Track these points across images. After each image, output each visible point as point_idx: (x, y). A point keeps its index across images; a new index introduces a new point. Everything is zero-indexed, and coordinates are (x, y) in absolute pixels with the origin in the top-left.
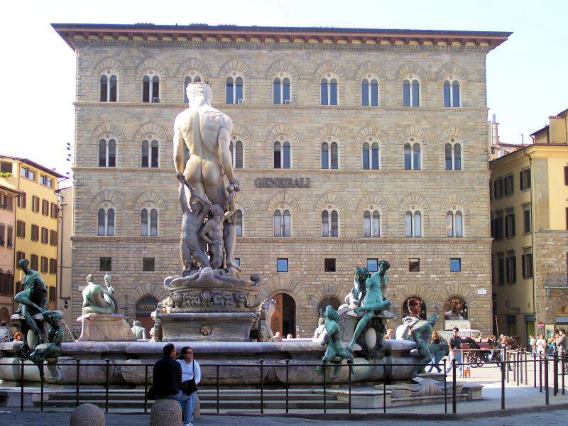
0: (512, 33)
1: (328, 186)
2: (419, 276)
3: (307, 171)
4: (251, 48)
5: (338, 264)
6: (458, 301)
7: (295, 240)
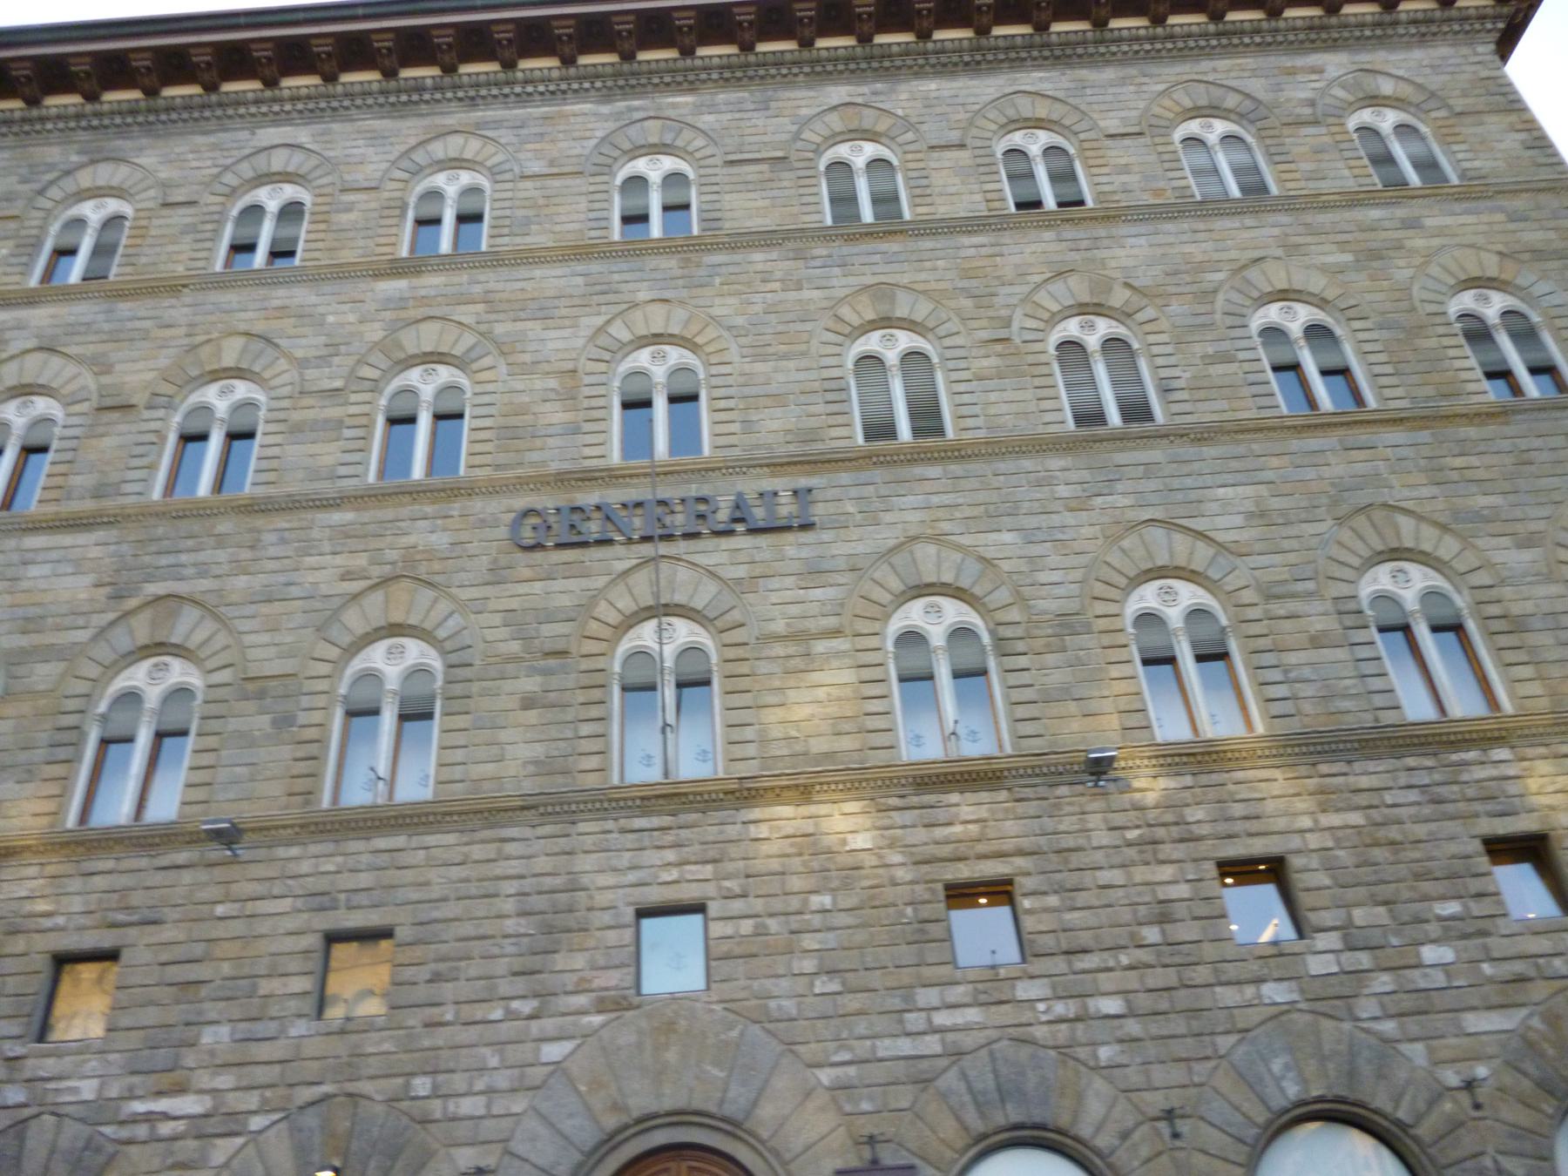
1: (908, 511)
4: (523, 99)
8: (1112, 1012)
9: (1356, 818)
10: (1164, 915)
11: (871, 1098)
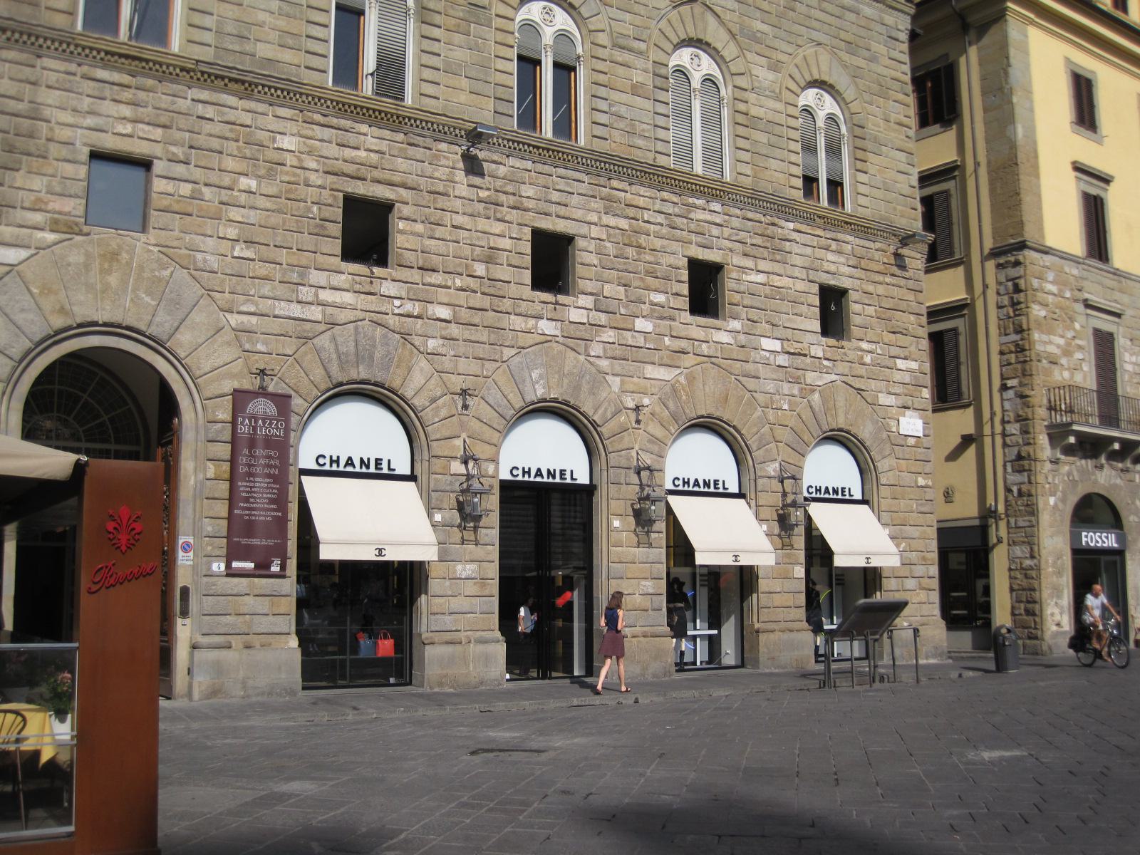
2: (723, 337)
8: (443, 317)
9: (624, 223)
10: (489, 261)
11: (265, 343)
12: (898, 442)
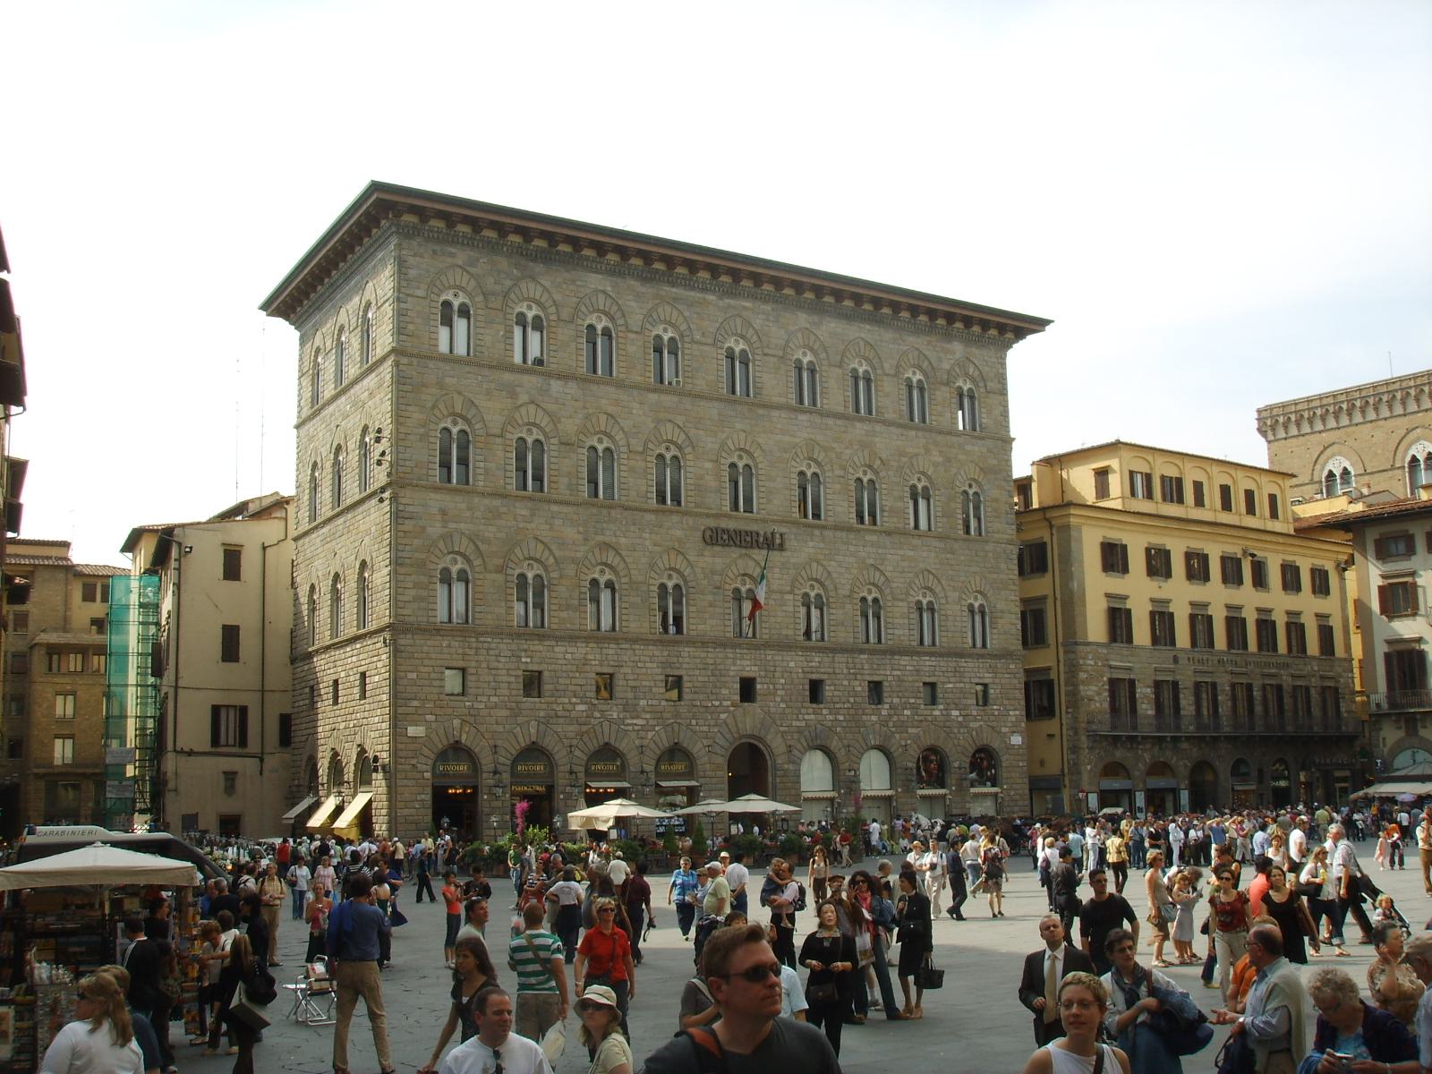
0: (1038, 324)
2: (937, 713)
3: (782, 521)
4: (693, 288)
5: (828, 690)
6: (983, 755)
7: (767, 645)
9: (899, 673)
12: (1010, 747)
